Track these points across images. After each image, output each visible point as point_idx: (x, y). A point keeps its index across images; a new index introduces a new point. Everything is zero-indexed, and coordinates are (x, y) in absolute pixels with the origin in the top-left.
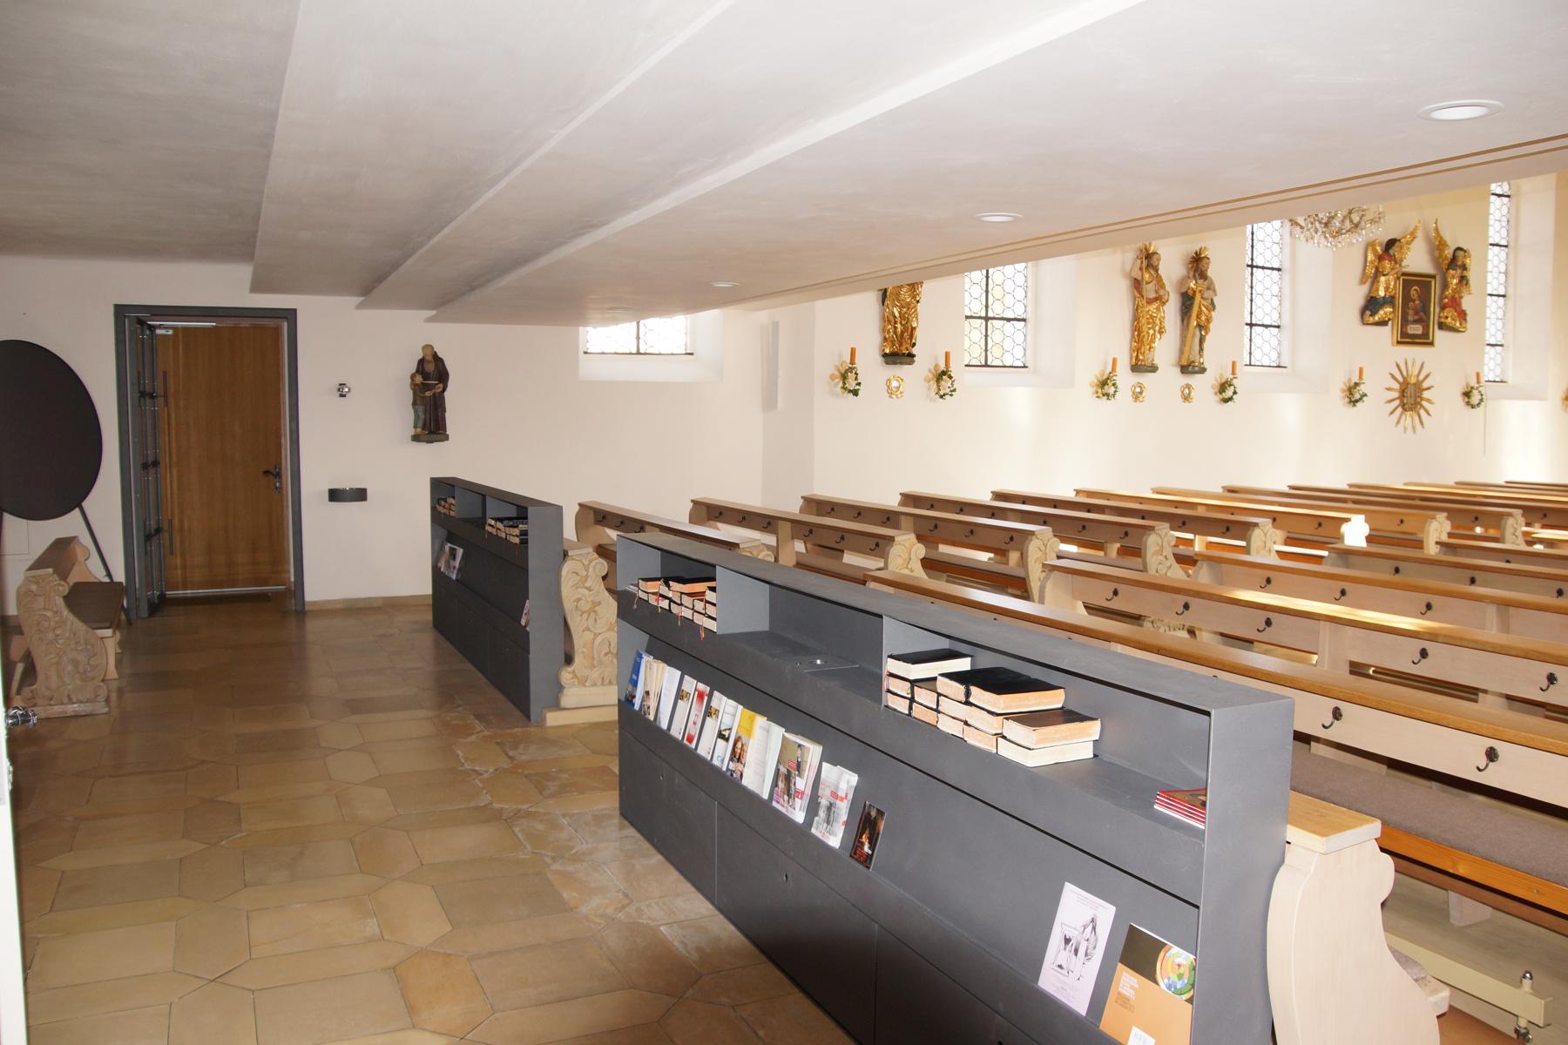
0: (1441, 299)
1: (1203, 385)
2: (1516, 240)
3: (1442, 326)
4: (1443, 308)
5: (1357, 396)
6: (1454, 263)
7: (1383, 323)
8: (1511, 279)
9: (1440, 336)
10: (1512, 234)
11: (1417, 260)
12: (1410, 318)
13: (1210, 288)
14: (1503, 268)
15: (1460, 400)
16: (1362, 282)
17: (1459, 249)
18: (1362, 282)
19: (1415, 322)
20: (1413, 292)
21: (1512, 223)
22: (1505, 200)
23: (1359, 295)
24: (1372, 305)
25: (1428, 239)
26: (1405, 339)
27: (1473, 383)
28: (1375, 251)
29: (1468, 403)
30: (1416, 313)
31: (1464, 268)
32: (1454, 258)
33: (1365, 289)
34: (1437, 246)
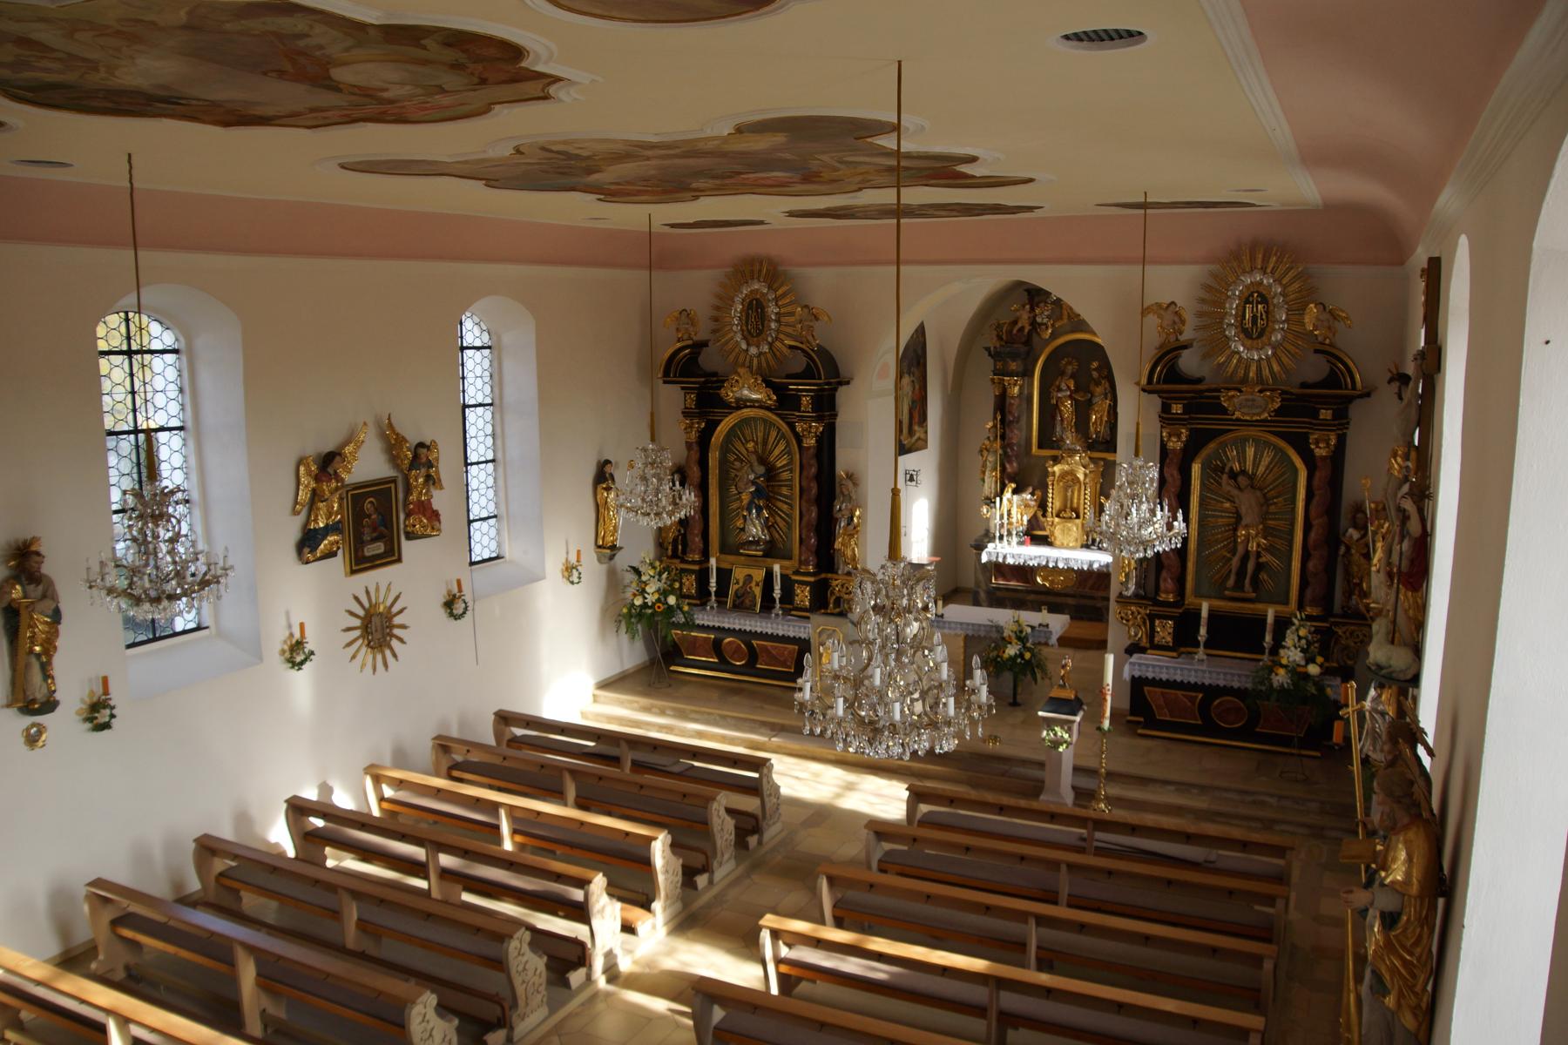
0: (406, 505)
1: (64, 723)
2: (501, 398)
3: (410, 536)
4: (408, 516)
5: (299, 659)
6: (417, 461)
7: (332, 554)
8: (499, 442)
9: (407, 547)
10: (496, 390)
11: (368, 465)
12: (367, 538)
13: (49, 593)
14: (489, 429)
15: (442, 613)
16: (295, 513)
17: (421, 445)
18: (295, 513)
19: (374, 540)
20: (367, 506)
21: (497, 377)
22: (486, 352)
23: (292, 529)
24: (308, 543)
25: (383, 436)
26: (360, 563)
27: (455, 590)
28: (309, 473)
29: (451, 615)
30: (375, 530)
31: (430, 465)
32: (416, 456)
33: (302, 518)
34: (392, 443)
